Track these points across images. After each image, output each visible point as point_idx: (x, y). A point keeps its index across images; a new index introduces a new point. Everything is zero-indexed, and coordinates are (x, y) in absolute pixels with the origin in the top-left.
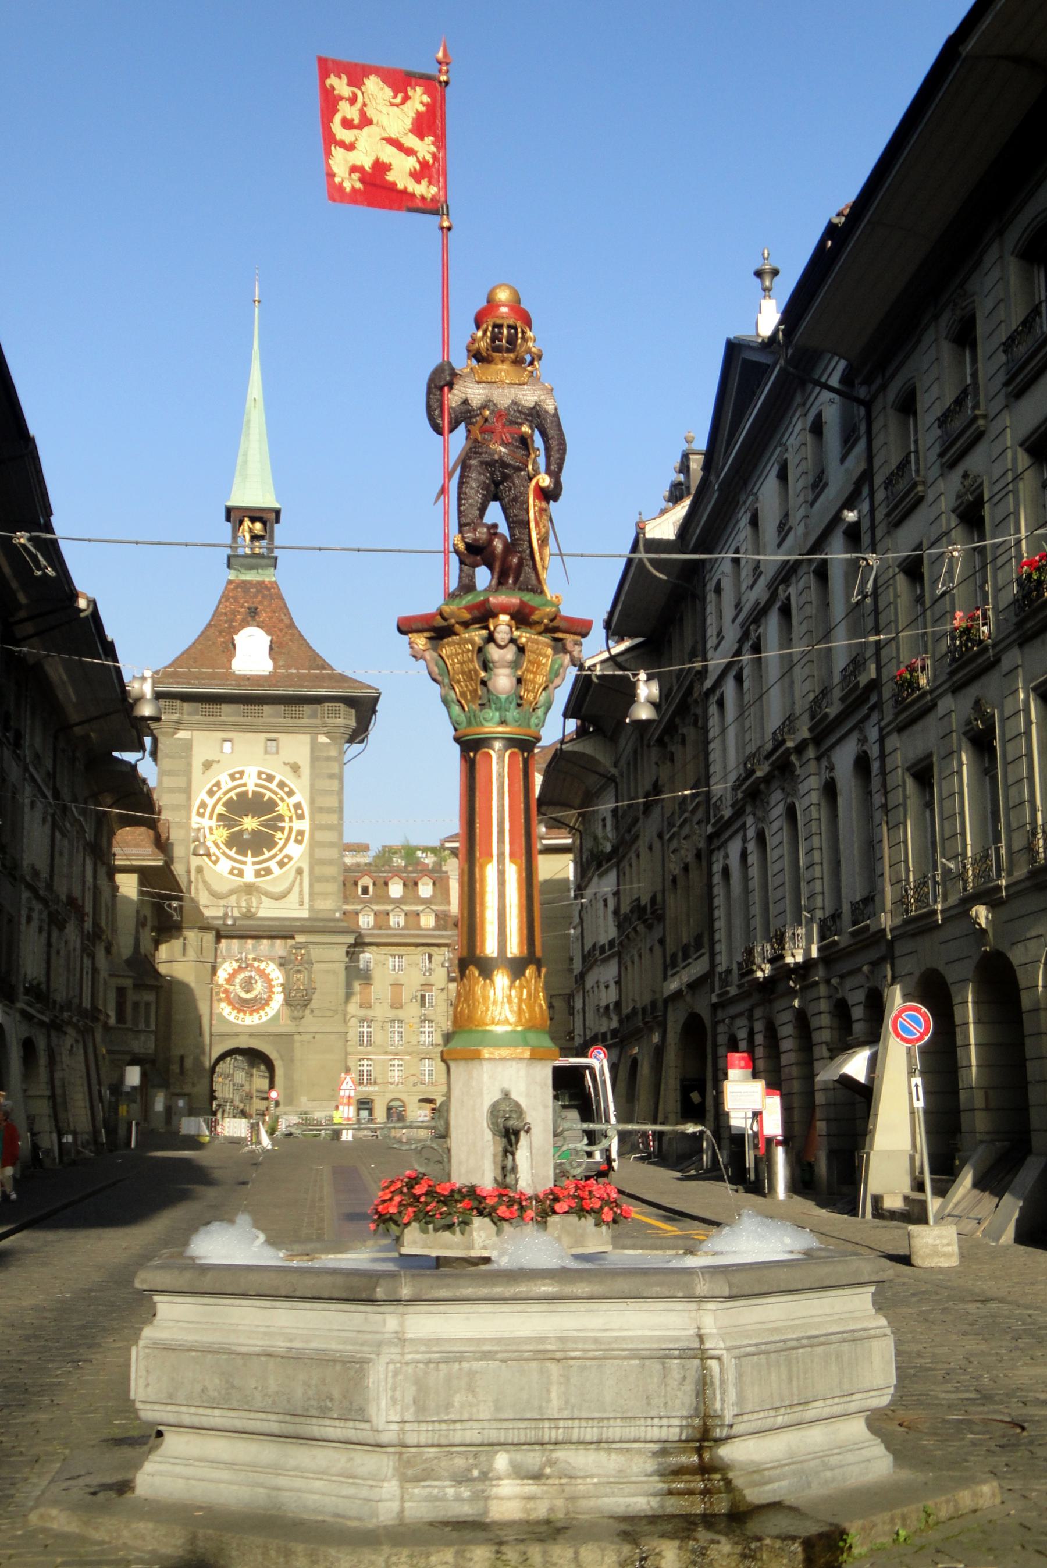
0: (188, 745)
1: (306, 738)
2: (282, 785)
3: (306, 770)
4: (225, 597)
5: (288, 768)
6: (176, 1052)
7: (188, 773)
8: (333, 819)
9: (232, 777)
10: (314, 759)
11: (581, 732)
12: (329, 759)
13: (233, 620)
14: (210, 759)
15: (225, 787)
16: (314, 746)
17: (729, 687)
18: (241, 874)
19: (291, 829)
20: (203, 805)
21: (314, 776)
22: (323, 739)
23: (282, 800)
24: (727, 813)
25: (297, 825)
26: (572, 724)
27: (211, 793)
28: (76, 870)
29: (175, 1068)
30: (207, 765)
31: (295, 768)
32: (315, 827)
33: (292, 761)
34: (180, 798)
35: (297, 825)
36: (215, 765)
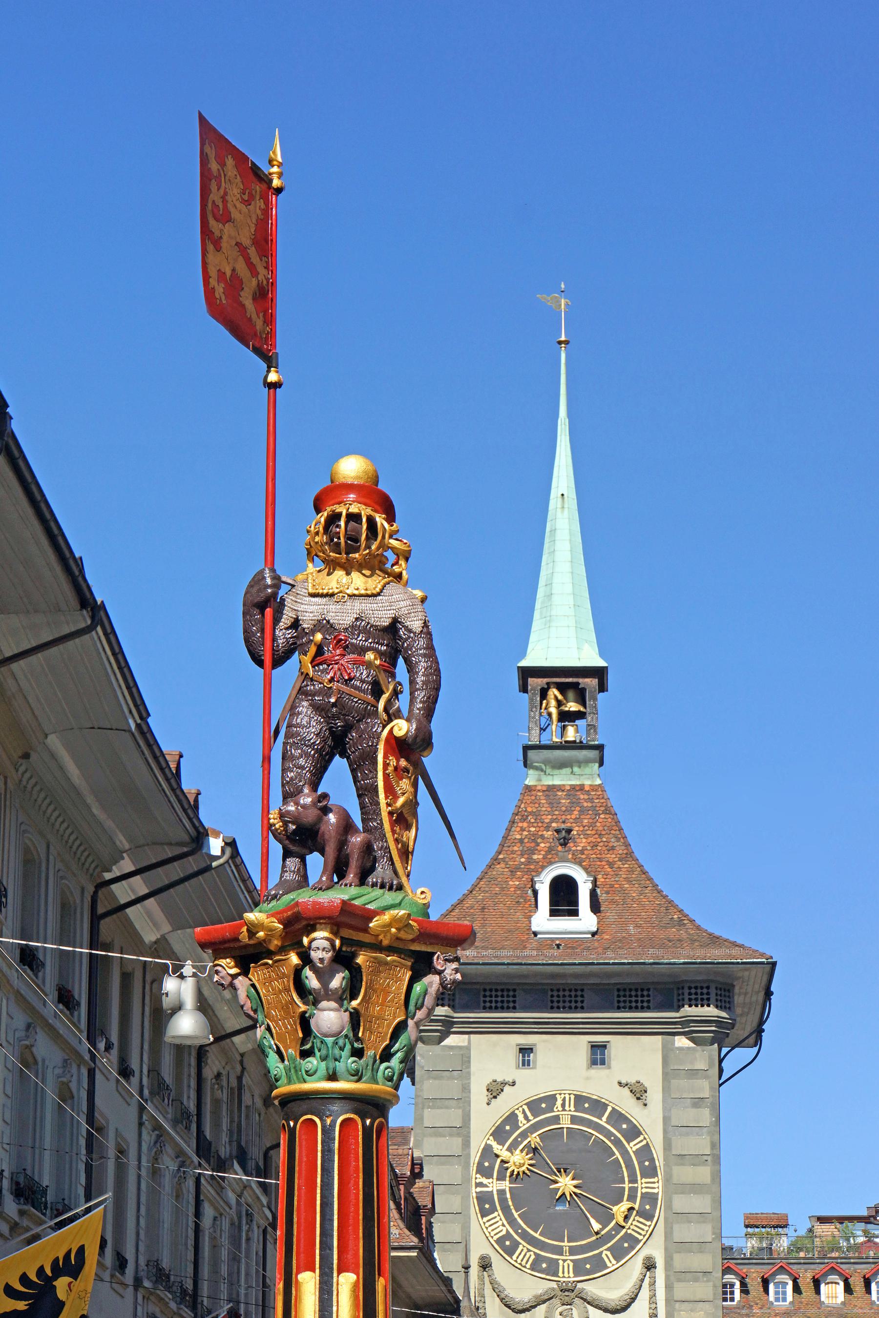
0: (465, 1056)
3: (655, 1096)
5: (626, 1091)
7: (463, 1101)
10: (667, 1076)
12: (693, 1073)
13: (532, 851)
14: (499, 1079)
15: (523, 1125)
18: (553, 1269)
22: (682, 1042)
25: (643, 1185)
30: (495, 1090)
31: (639, 1092)
32: (672, 1187)
33: (632, 1080)
34: (454, 1145)
35: (643, 1185)
36: (507, 1089)
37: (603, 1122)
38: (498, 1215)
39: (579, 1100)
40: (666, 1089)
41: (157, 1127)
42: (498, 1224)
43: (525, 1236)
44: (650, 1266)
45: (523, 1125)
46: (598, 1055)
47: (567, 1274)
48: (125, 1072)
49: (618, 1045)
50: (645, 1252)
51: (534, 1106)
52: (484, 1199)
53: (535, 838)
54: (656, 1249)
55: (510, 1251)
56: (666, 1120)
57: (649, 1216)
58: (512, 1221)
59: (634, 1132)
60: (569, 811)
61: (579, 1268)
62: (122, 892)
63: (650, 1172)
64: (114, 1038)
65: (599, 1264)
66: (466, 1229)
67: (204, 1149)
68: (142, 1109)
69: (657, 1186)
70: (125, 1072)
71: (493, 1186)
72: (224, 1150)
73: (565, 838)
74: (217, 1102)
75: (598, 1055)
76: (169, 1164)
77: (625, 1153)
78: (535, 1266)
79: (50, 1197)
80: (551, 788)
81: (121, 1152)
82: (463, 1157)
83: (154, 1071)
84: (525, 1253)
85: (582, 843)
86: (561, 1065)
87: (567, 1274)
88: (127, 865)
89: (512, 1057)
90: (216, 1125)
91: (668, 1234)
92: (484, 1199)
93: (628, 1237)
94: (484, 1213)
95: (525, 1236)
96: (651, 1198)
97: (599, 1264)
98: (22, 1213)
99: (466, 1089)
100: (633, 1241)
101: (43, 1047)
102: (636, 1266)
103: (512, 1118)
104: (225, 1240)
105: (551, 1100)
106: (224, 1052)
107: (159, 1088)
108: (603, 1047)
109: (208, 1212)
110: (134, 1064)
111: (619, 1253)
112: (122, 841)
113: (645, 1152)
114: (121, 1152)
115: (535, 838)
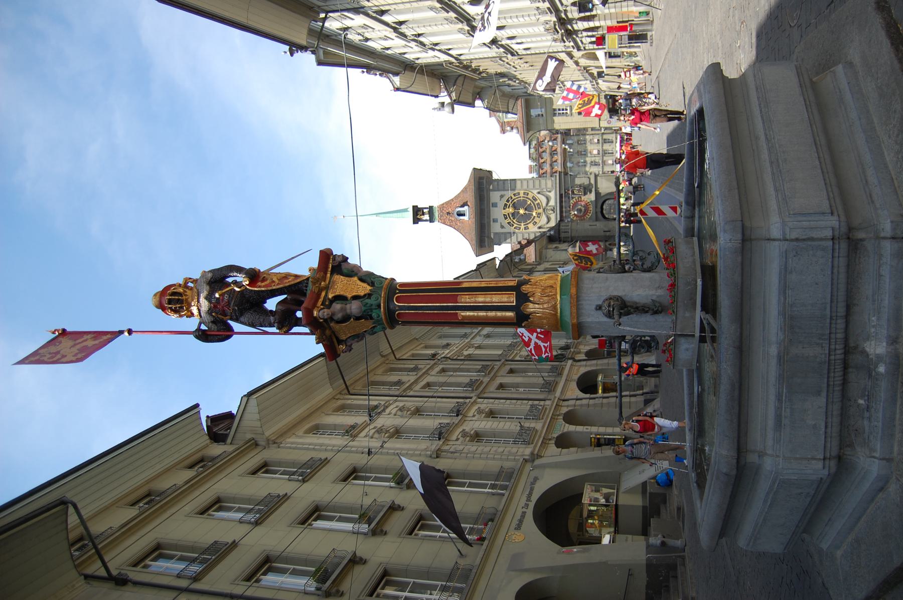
0: (495, 234)
2: (508, 201)
4: (444, 223)
6: (603, 234)
7: (505, 234)
9: (506, 218)
10: (498, 190)
16: (493, 190)
18: (539, 214)
21: (504, 190)
22: (491, 187)
24: (502, 50)
25: (522, 195)
26: (478, 103)
29: (608, 234)
30: (502, 227)
31: (502, 196)
35: (522, 195)
42: (530, 226)
46: (495, 205)
47: (541, 211)
51: (506, 218)
52: (525, 229)
63: (519, 194)
69: (522, 192)
71: (523, 227)
73: (448, 213)
75: (495, 205)
84: (536, 220)
86: (498, 213)
87: (541, 211)
89: (496, 224)
97: (538, 204)
111: (535, 200)
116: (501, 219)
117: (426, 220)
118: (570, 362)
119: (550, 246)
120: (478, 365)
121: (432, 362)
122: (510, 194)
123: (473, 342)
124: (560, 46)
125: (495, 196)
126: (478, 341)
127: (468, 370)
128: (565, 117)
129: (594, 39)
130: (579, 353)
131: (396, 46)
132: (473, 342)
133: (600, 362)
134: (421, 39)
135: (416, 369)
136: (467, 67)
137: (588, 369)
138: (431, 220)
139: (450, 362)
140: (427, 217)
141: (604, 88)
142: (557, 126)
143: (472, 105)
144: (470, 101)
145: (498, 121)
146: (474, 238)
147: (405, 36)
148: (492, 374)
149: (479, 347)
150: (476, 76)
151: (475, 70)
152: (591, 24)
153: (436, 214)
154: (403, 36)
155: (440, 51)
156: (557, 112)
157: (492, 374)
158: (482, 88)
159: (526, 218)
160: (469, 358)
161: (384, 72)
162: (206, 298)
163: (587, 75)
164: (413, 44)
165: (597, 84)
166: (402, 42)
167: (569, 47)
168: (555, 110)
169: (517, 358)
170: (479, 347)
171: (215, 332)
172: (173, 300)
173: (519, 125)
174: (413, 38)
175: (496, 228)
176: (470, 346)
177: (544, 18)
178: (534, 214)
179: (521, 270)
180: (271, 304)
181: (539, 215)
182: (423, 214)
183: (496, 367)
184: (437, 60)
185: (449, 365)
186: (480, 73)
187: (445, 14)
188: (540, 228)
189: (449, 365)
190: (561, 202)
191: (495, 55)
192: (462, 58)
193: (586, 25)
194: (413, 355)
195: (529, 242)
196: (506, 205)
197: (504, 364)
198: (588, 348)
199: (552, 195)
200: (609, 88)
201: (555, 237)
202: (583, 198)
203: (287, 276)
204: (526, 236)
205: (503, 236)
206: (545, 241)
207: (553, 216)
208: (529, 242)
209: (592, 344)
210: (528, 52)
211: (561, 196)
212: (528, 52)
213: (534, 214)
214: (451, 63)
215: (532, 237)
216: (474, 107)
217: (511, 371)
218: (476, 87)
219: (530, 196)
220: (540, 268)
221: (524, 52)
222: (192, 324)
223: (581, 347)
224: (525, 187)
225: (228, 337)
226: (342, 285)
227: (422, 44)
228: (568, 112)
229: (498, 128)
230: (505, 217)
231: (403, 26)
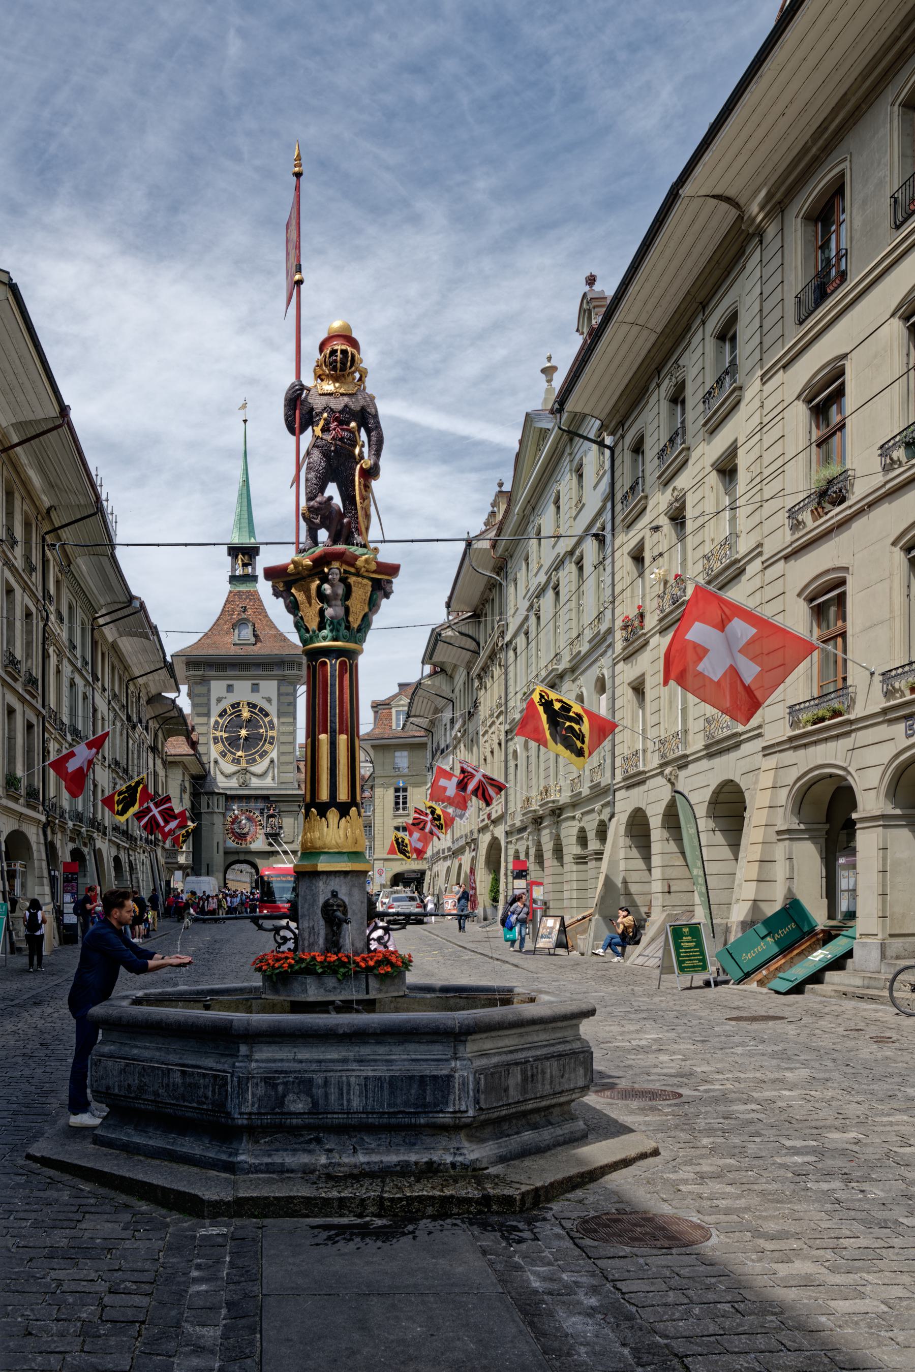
1: (274, 683)
2: (261, 710)
7: (208, 705)
8: (291, 729)
10: (280, 695)
11: (434, 673)
12: (287, 694)
13: (232, 615)
15: (229, 712)
17: (521, 641)
19: (267, 735)
20: (217, 722)
23: (261, 718)
25: (270, 733)
26: (428, 669)
27: (221, 715)
28: (143, 762)
30: (219, 700)
31: (269, 700)
37: (256, 711)
38: (220, 744)
39: (248, 704)
40: (279, 700)
41: (115, 710)
43: (229, 751)
44: (272, 761)
45: (229, 712)
46: (255, 688)
47: (243, 764)
48: (104, 690)
49: (263, 684)
50: (271, 756)
51: (233, 706)
52: (215, 738)
53: (233, 610)
54: (274, 755)
55: (224, 756)
56: (278, 710)
57: (272, 744)
58: (225, 746)
59: (267, 715)
60: (245, 600)
61: (248, 762)
62: (101, 621)
63: (272, 728)
64: (100, 677)
65: (254, 760)
66: (209, 749)
67: (129, 718)
68: (109, 703)
70: (104, 690)
71: (218, 734)
72: (135, 719)
74: (132, 702)
75: (255, 688)
76: (119, 724)
77: (264, 722)
78: (233, 761)
79: (82, 735)
80: (239, 592)
81: (103, 719)
82: (208, 724)
83: (113, 690)
85: (250, 612)
86: (242, 691)
88: (104, 611)
90: (132, 711)
91: (278, 750)
92: (215, 738)
93: (264, 751)
94: (215, 743)
95: (229, 751)
96: (272, 738)
97: (254, 760)
98: (73, 740)
99: (209, 700)
100: (266, 752)
101: (78, 680)
102: (266, 762)
103: (225, 711)
104: (136, 752)
105: (238, 704)
106: (135, 684)
107: (115, 695)
108: (257, 684)
109: (131, 742)
110: (106, 687)
111: (261, 756)
112: (102, 602)
113: (271, 722)
114: (103, 719)
115: (233, 610)
116: (232, 699)
117: (234, 569)
118: (43, 818)
119: (187, 778)
120: (37, 673)
121: (40, 594)
122: (272, 709)
123: (65, 662)
124: (516, 805)
125: (270, 688)
126: (67, 669)
127: (28, 656)
128: (393, 804)
129: (522, 857)
130: (53, 833)
131: (541, 554)
132: (65, 662)
133: (44, 864)
134: (550, 593)
135: (31, 569)
136: (492, 656)
137: (34, 847)
138: (233, 579)
139: (41, 624)
140: (239, 572)
141: (436, 868)
142: (378, 791)
143: (428, 657)
144: (435, 659)
145: (393, 698)
146: (204, 652)
147: (557, 569)
148: (28, 697)
149: (58, 672)
150: (475, 671)
151: (485, 669)
152: (548, 854)
153: (243, 588)
154: (558, 565)
155: (526, 618)
156: (401, 794)
157: (28, 697)
158: (451, 677)
159: (233, 742)
160: (46, 656)
161: (497, 525)
162: (346, 406)
163: (462, 842)
164: (542, 578)
165: (445, 858)
166: (547, 561)
167: (513, 819)
168: (405, 790)
169: (46, 735)
170: (58, 672)
171: (298, 411)
172: (340, 360)
173: (387, 733)
174: (554, 579)
175: (217, 687)
176: (60, 654)
177: (565, 783)
178: (240, 753)
179: (156, 735)
180: (332, 490)
181: (237, 761)
182: (245, 565)
183: (33, 702)
184: (511, 611)
185: (37, 624)
186: (479, 677)
187: (588, 634)
188: (216, 762)
189: (37, 624)
190: (257, 797)
191: (511, 704)
192: (511, 653)
193: (548, 847)
194: (48, 561)
195: (193, 745)
196: (254, 706)
197: (38, 714)
198: (58, 845)
199: (268, 782)
200: (437, 875)
201: (200, 782)
202: (262, 832)
203: (368, 516)
204: (202, 740)
205: (204, 700)
206: (196, 770)
207: (234, 783)
208: (193, 745)
209: (63, 852)
210: (510, 757)
211: (265, 798)
212: (510, 757)
213: (240, 753)
214: (502, 634)
215: (201, 749)
216: (423, 663)
217: (30, 726)
218: (455, 667)
219: (267, 747)
220: (159, 762)
221: (510, 750)
222: (308, 380)
223: (59, 836)
224: (284, 739)
225: (292, 430)
226: (361, 590)
227: (541, 592)
228: (401, 811)
229: (382, 696)
230: (235, 706)
231: (573, 566)
